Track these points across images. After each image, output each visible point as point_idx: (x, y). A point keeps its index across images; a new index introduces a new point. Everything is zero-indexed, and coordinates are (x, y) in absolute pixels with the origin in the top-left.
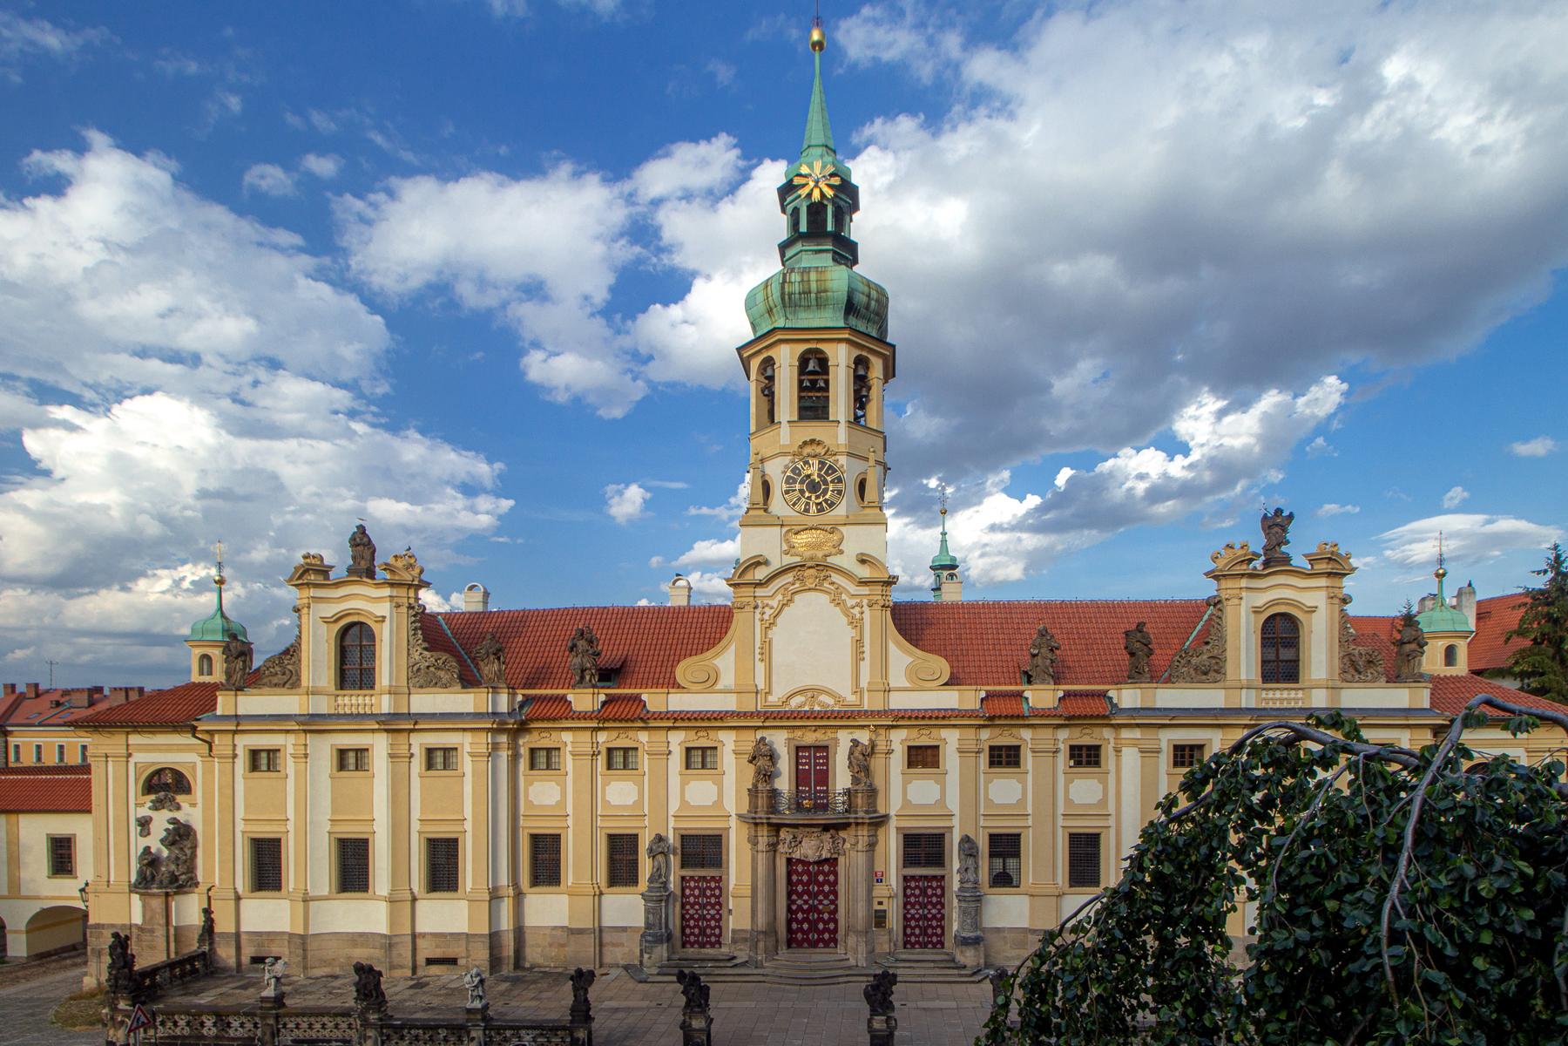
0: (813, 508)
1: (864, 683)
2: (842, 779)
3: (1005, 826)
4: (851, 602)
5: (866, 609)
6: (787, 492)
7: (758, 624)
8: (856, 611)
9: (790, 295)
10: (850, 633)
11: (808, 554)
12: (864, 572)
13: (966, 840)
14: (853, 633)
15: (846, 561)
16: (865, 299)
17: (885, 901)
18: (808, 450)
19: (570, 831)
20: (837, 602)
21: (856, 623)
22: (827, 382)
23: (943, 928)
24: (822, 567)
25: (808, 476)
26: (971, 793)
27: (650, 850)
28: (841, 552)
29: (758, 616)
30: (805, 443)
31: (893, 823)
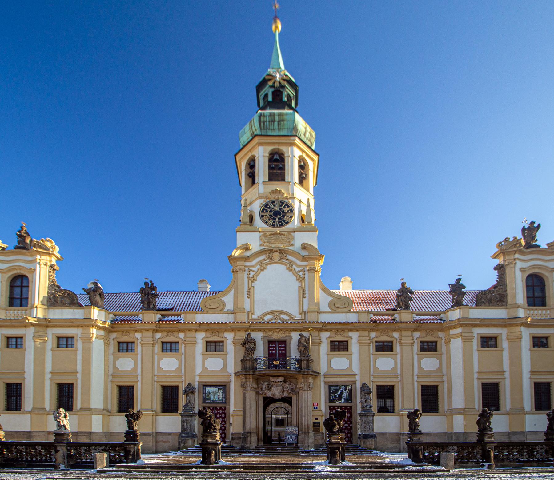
2: (294, 353)
3: (386, 381)
6: (262, 216)
8: (301, 273)
11: (273, 246)
12: (304, 253)
13: (364, 386)
17: (319, 418)
18: (273, 196)
19: (139, 383)
20: (290, 269)
22: (284, 166)
23: (351, 434)
26: (365, 364)
27: (185, 391)
28: (292, 245)
29: (246, 275)
31: (322, 379)
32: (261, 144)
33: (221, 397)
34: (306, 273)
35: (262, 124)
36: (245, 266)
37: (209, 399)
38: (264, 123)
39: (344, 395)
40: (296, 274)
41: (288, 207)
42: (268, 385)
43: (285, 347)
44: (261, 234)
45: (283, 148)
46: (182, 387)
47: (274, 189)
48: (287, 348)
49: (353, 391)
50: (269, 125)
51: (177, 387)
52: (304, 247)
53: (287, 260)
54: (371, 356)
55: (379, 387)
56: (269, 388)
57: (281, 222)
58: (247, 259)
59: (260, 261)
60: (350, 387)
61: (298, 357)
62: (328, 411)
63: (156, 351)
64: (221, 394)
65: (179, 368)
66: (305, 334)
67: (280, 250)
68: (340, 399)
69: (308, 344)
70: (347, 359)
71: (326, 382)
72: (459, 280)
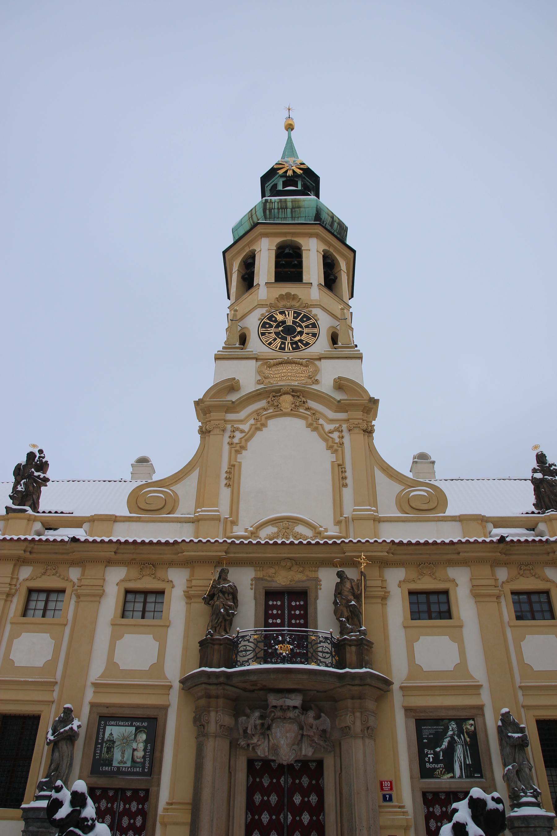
1: (348, 510)
4: (328, 427)
5: (346, 434)
6: (263, 334)
7: (226, 448)
8: (335, 435)
10: (328, 457)
13: (507, 723)
14: (333, 457)
20: (314, 426)
21: (335, 448)
25: (284, 322)
26: (498, 656)
28: (317, 382)
29: (226, 440)
30: (282, 297)
31: (398, 701)
32: (266, 235)
33: (140, 754)
34: (346, 434)
35: (268, 211)
36: (225, 421)
37: (109, 762)
38: (270, 210)
39: (459, 752)
40: (325, 437)
41: (309, 319)
42: (262, 717)
43: (305, 608)
44: (259, 363)
45: (301, 241)
46: (49, 718)
48: (310, 610)
49: (480, 737)
50: (278, 213)
51: (35, 719)
52: (341, 384)
53: (308, 409)
54: (509, 632)
55: (542, 724)
56: (265, 730)
59: (257, 413)
60: (469, 726)
61: (337, 636)
62: (422, 810)
63: (11, 613)
64: (141, 746)
65: (52, 664)
67: (293, 391)
68: (450, 769)
69: (358, 598)
70: (453, 639)
71: (408, 710)
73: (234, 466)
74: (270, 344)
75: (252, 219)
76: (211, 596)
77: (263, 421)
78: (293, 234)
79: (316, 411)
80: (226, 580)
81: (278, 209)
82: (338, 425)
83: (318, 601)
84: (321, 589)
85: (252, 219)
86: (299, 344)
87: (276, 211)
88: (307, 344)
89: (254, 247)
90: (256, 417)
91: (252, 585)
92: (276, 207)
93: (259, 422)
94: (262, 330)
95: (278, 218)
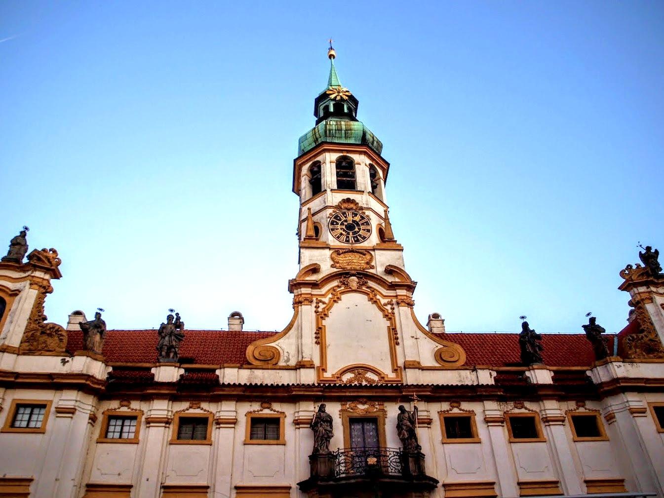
0: (351, 239)
1: (400, 362)
5: (395, 306)
6: (333, 230)
8: (389, 307)
9: (330, 130)
12: (390, 279)
14: (388, 323)
15: (379, 270)
16: (371, 139)
18: (346, 205)
21: (389, 317)
22: (354, 173)
24: (364, 276)
25: (346, 221)
28: (372, 267)
34: (395, 306)
36: (312, 295)
44: (332, 251)
47: (345, 198)
50: (336, 133)
52: (390, 270)
57: (356, 237)
58: (315, 285)
59: (333, 289)
66: (407, 407)
67: (359, 274)
69: (413, 423)
72: (592, 320)
73: (320, 328)
74: (338, 237)
75: (315, 136)
76: (316, 423)
77: (339, 296)
78: (348, 151)
79: (375, 289)
80: (324, 412)
81: (336, 130)
82: (390, 300)
83: (386, 426)
84: (386, 418)
85: (315, 136)
86: (359, 237)
87: (334, 131)
88: (364, 238)
89: (319, 158)
90: (331, 291)
91: (340, 415)
92: (334, 129)
93: (336, 297)
94: (331, 227)
95: (336, 137)
